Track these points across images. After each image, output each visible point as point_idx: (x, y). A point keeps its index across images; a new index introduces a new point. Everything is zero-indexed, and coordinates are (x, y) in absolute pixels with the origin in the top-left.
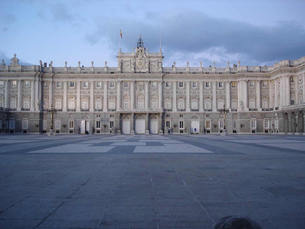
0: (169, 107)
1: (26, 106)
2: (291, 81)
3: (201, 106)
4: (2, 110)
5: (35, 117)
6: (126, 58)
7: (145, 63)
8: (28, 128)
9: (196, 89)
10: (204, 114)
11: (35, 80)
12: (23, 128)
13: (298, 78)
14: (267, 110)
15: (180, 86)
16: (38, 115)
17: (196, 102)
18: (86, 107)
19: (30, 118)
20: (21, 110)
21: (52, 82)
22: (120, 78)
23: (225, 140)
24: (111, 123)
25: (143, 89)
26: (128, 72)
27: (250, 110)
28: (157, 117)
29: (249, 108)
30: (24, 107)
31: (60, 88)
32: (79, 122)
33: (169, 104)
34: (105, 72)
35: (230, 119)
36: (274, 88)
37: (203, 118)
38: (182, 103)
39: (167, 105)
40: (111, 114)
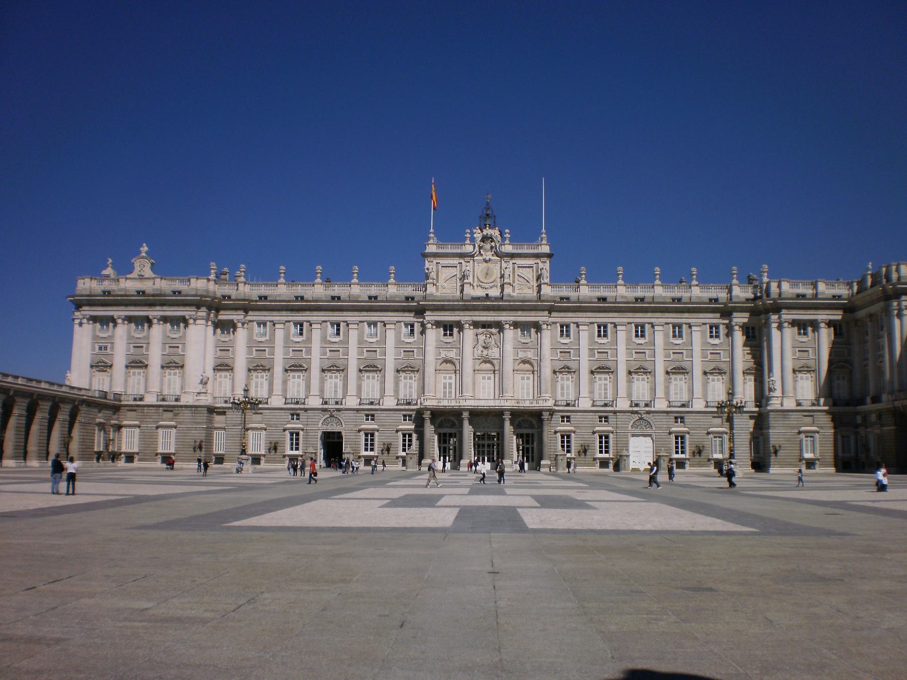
0: (568, 394)
1: (169, 388)
3: (660, 392)
4: (106, 398)
5: (192, 420)
7: (501, 272)
8: (175, 450)
9: (646, 342)
10: (667, 412)
11: (195, 320)
12: (160, 450)
14: (848, 404)
15: (599, 336)
16: (202, 415)
17: (643, 380)
18: (336, 392)
19: (180, 423)
20: (158, 401)
21: (243, 324)
23: (752, 491)
24: (678, 447)
25: (493, 343)
26: (453, 296)
27: (799, 404)
28: (535, 422)
29: (796, 397)
30: (165, 392)
31: (263, 339)
32: (316, 434)
33: (568, 387)
35: (742, 430)
36: (865, 342)
37: (664, 426)
38: (606, 385)
39: (562, 388)
40: (404, 413)
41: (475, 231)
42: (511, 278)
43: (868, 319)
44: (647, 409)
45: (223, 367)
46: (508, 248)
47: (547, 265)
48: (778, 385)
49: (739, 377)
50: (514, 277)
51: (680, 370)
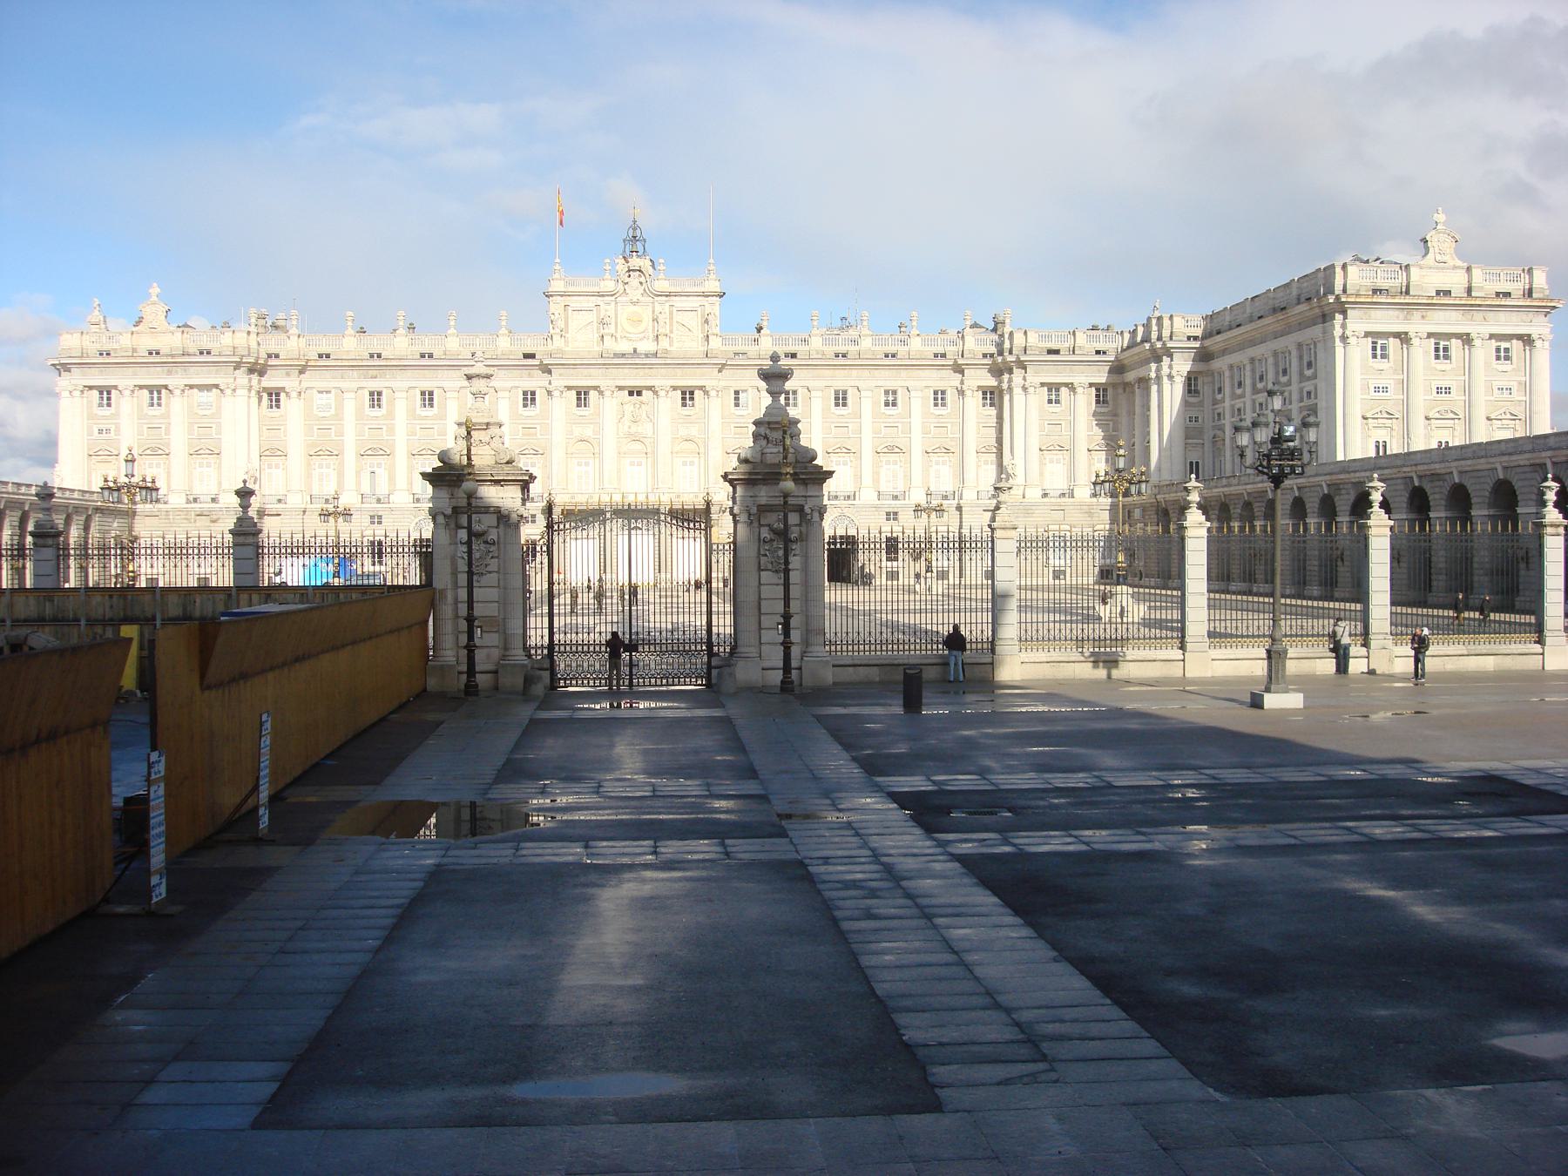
2: (1190, 391)
3: (867, 479)
6: (582, 298)
10: (876, 507)
13: (1213, 383)
20: (188, 502)
22: (560, 375)
25: (644, 415)
30: (198, 490)
34: (499, 353)
41: (617, 261)
42: (668, 326)
43: (1136, 386)
44: (850, 502)
45: (273, 452)
46: (662, 285)
47: (716, 309)
48: (1019, 471)
49: (971, 458)
50: (671, 325)
51: (891, 450)
